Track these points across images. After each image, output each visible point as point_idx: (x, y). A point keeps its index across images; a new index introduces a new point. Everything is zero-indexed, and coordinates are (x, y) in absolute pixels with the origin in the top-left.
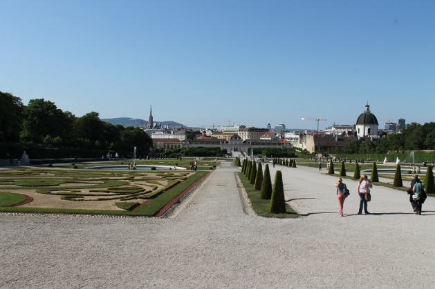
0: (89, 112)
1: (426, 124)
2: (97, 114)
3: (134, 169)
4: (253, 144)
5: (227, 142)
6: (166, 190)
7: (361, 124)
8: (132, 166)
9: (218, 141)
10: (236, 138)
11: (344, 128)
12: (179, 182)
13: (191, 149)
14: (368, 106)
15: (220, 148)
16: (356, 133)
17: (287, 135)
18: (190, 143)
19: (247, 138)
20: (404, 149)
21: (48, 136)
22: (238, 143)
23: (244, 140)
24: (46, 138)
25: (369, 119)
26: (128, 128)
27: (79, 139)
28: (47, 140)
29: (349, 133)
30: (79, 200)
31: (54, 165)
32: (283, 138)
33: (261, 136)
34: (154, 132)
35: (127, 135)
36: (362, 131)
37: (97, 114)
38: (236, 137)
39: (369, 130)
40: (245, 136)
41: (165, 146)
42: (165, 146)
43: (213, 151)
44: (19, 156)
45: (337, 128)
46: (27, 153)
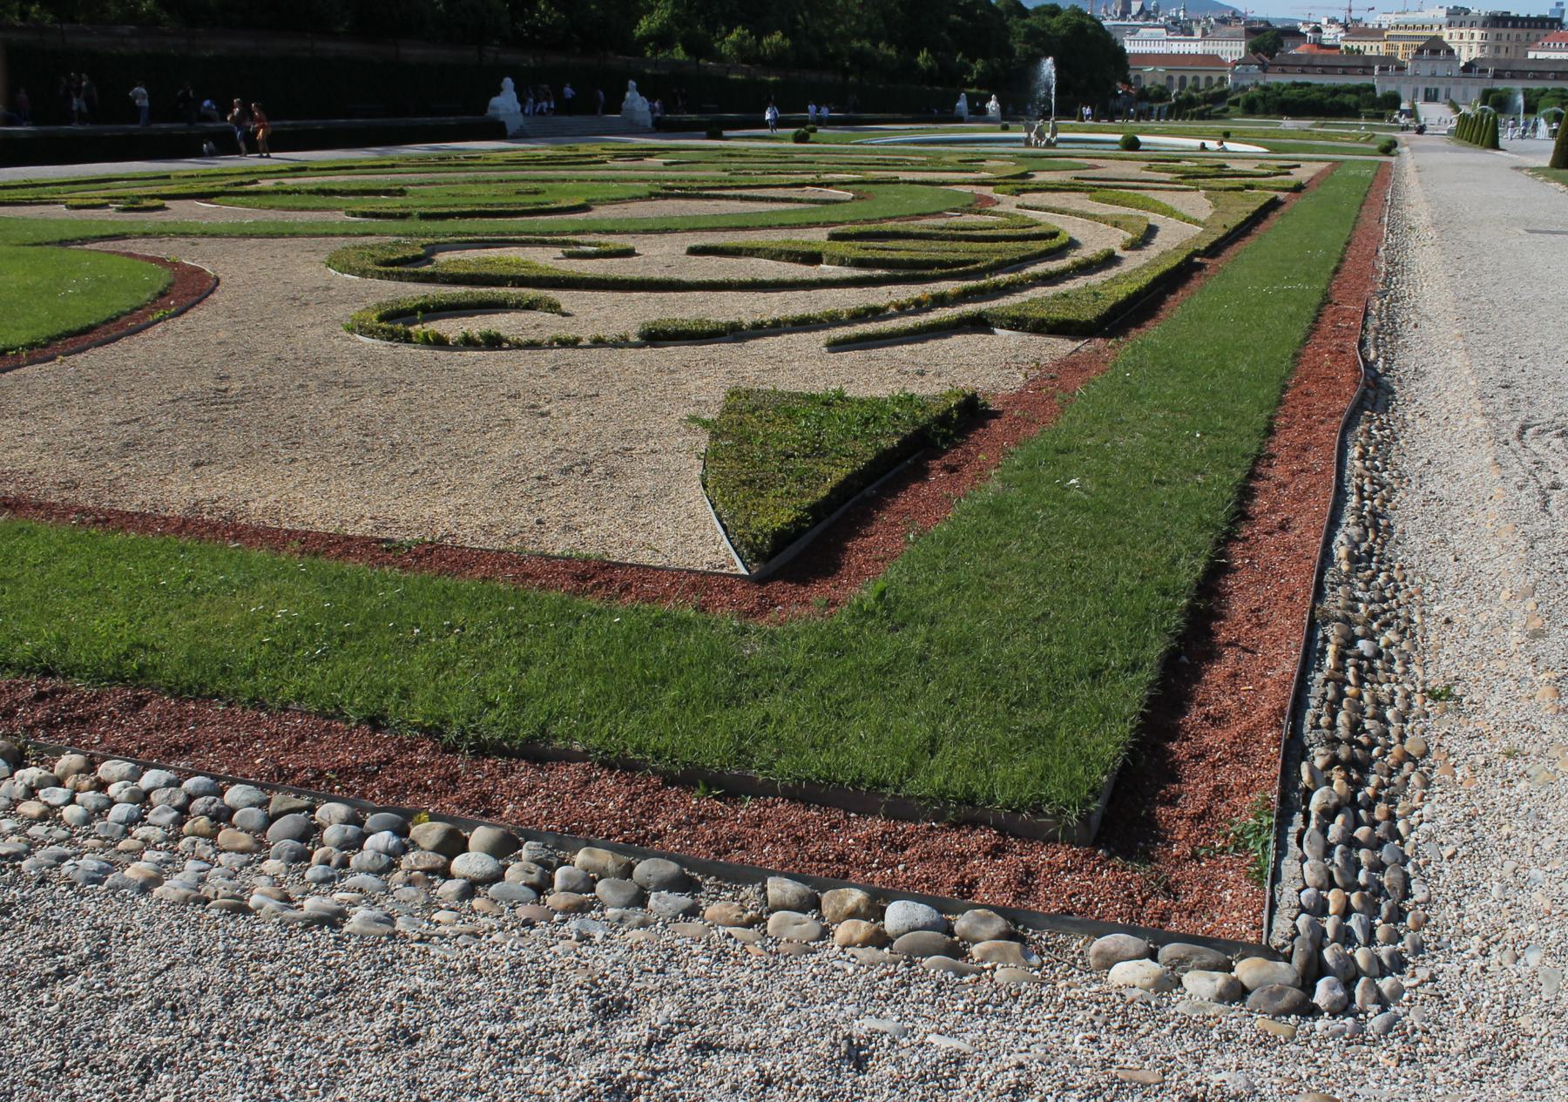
3: (1049, 144)
4: (1498, 75)
5: (1401, 68)
6: (1215, 250)
8: (1040, 135)
9: (1366, 65)
10: (1435, 52)
12: (1274, 204)
13: (1266, 88)
15: (1373, 88)
18: (1264, 68)
21: (738, 30)
22: (1441, 69)
24: (733, 37)
26: (1037, 11)
27: (855, 44)
28: (738, 46)
30: (468, 343)
31: (726, 133)
33: (1530, 44)
34: (1134, 30)
38: (1435, 48)
40: (1468, 46)
41: (1170, 78)
42: (1170, 78)
43: (1350, 99)
44: (615, 104)
46: (642, 91)
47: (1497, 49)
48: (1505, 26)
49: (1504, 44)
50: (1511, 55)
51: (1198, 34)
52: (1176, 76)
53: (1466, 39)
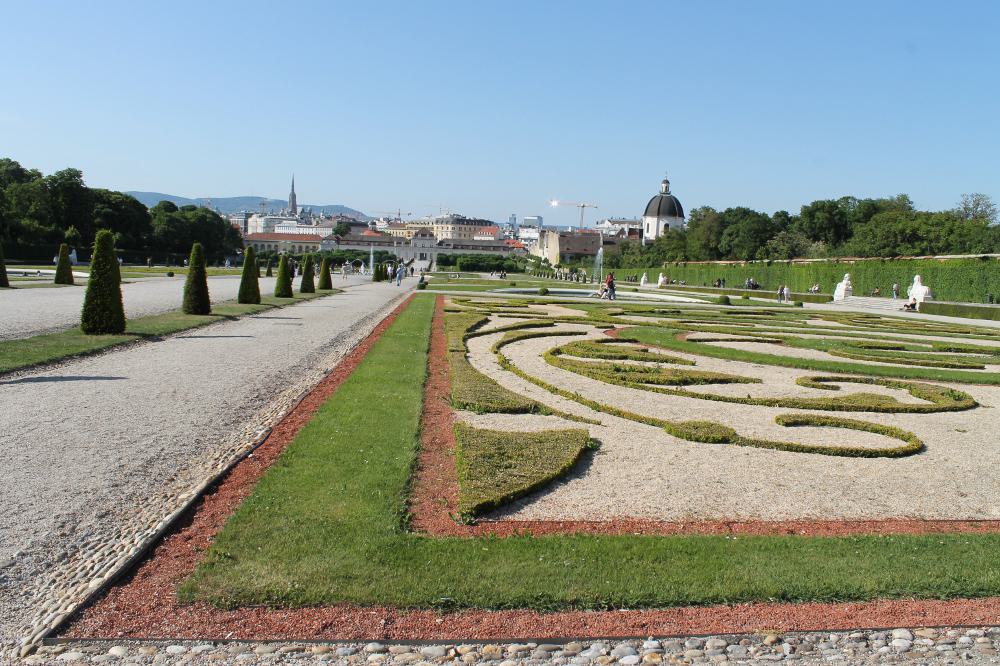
0: (63, 168)
1: (729, 211)
2: (78, 174)
7: (652, 215)
9: (390, 241)
11: (620, 223)
14: (667, 182)
16: (641, 231)
17: (524, 234)
18: (338, 241)
19: (450, 237)
20: (687, 259)
22: (427, 244)
23: (440, 239)
25: (668, 207)
26: (183, 209)
29: (632, 232)
32: (517, 238)
35: (172, 221)
36: (653, 228)
37: (78, 174)
38: (425, 233)
39: (667, 226)
42: (293, 246)
45: (613, 222)
47: (460, 235)
48: (463, 224)
49: (463, 233)
50: (467, 238)
51: (314, 223)
52: (297, 246)
53: (445, 229)
